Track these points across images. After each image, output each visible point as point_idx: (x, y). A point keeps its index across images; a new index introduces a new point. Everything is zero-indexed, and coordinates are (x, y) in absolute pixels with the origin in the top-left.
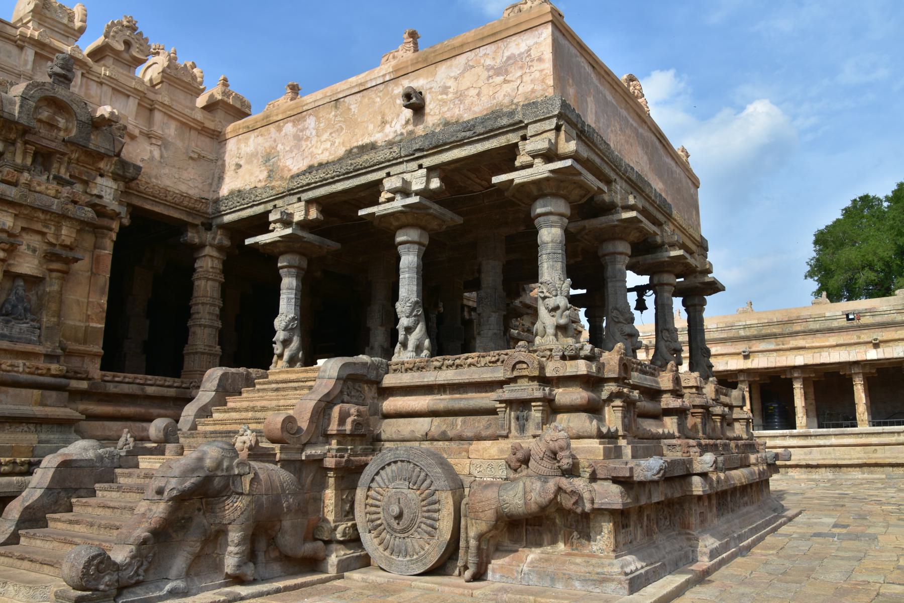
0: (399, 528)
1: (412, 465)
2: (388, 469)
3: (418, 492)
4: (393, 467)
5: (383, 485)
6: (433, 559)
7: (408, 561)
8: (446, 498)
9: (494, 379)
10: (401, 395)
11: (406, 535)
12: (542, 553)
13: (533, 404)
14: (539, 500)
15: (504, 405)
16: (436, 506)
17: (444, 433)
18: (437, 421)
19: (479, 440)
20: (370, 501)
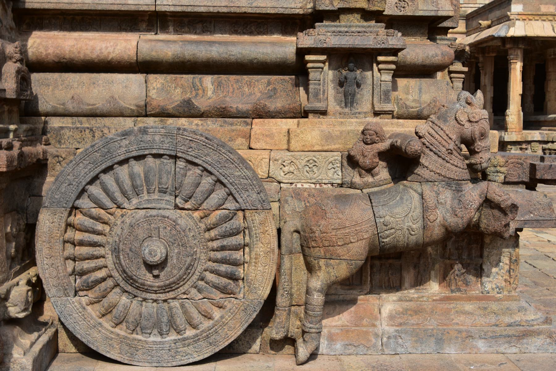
0: (158, 283)
1: (181, 164)
2: (123, 172)
3: (197, 215)
4: (138, 168)
5: (108, 203)
6: (234, 332)
7: (175, 342)
8: (262, 223)
9: (281, 11)
10: (62, 27)
11: (171, 295)
12: (400, 300)
13: (380, 58)
14: (452, 221)
15: (323, 58)
16: (238, 239)
17: (188, 103)
18: (157, 81)
19: (260, 117)
20: (79, 236)
